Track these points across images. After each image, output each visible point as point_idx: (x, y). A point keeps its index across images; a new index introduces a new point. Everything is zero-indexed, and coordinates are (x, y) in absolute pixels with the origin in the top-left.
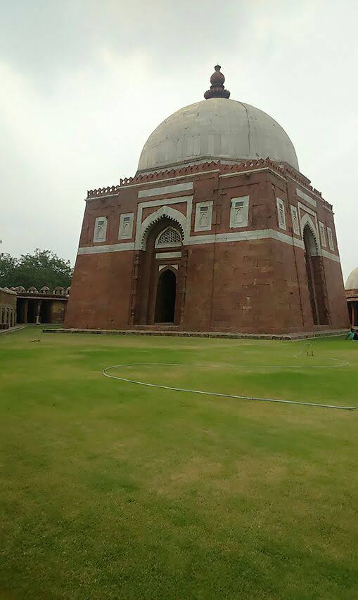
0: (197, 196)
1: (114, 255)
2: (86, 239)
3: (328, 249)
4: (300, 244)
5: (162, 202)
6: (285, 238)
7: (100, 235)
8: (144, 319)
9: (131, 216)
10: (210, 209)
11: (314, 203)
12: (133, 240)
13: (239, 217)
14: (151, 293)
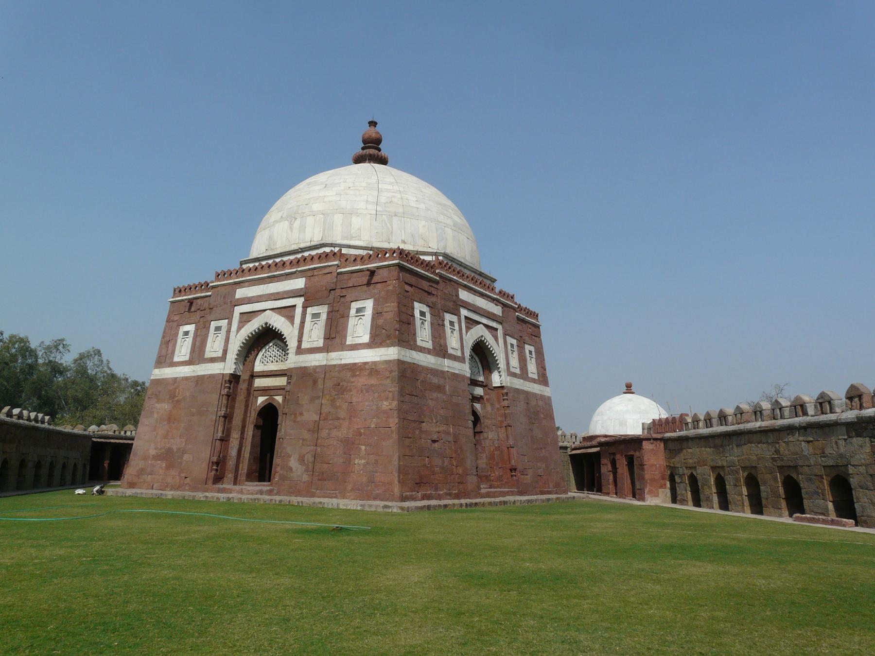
0: (310, 297)
1: (199, 380)
3: (524, 375)
4: (464, 369)
7: (183, 349)
8: (230, 476)
9: (224, 323)
10: (324, 317)
11: (497, 310)
12: (223, 359)
13: (359, 328)
14: (242, 437)
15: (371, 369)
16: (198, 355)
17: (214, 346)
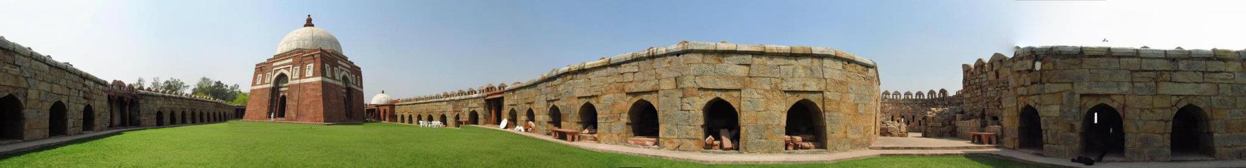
0: (294, 64)
2: (254, 84)
4: (341, 84)
5: (280, 68)
6: (330, 81)
7: (259, 82)
13: (309, 73)
15: (313, 84)
16: (263, 83)
17: (267, 80)
